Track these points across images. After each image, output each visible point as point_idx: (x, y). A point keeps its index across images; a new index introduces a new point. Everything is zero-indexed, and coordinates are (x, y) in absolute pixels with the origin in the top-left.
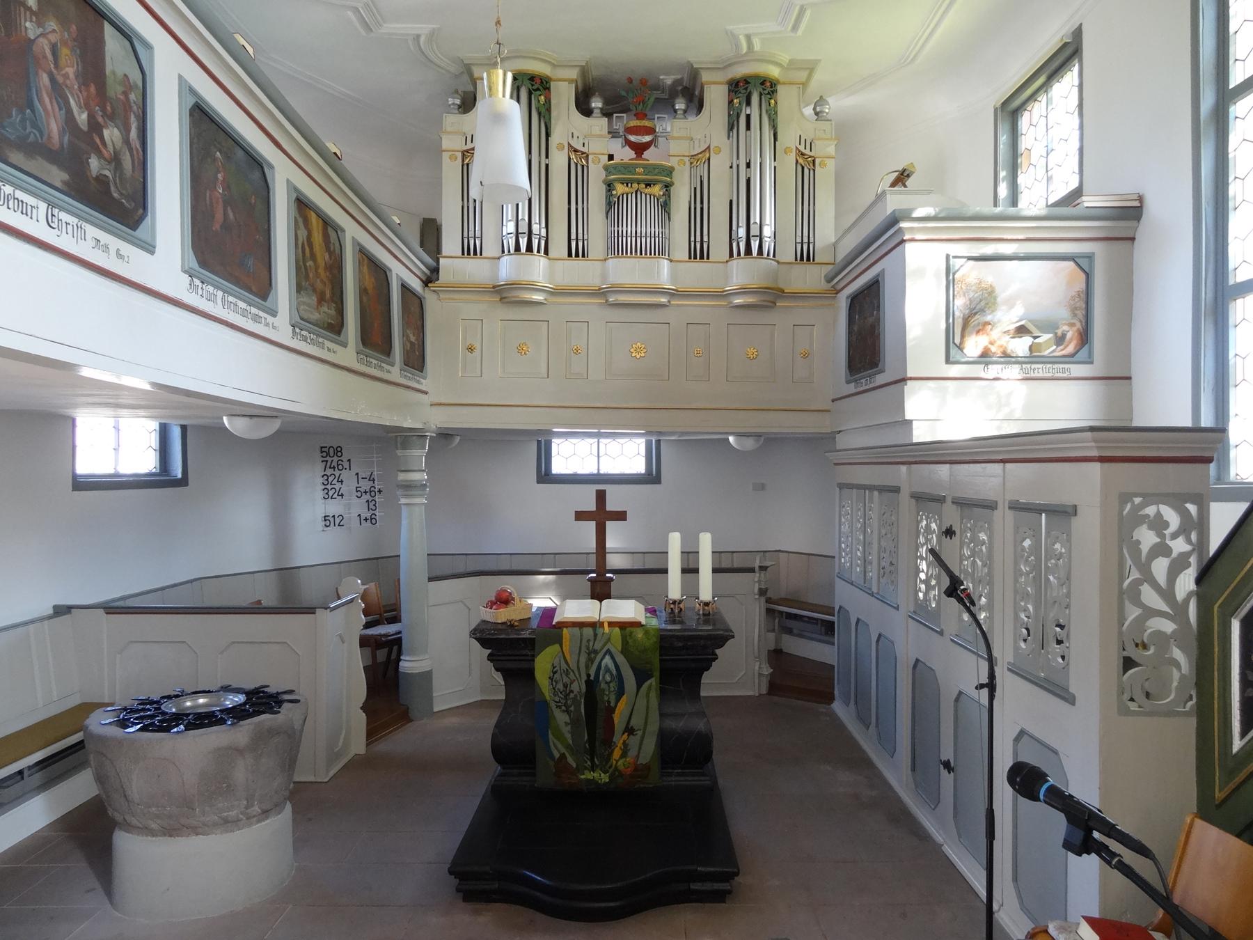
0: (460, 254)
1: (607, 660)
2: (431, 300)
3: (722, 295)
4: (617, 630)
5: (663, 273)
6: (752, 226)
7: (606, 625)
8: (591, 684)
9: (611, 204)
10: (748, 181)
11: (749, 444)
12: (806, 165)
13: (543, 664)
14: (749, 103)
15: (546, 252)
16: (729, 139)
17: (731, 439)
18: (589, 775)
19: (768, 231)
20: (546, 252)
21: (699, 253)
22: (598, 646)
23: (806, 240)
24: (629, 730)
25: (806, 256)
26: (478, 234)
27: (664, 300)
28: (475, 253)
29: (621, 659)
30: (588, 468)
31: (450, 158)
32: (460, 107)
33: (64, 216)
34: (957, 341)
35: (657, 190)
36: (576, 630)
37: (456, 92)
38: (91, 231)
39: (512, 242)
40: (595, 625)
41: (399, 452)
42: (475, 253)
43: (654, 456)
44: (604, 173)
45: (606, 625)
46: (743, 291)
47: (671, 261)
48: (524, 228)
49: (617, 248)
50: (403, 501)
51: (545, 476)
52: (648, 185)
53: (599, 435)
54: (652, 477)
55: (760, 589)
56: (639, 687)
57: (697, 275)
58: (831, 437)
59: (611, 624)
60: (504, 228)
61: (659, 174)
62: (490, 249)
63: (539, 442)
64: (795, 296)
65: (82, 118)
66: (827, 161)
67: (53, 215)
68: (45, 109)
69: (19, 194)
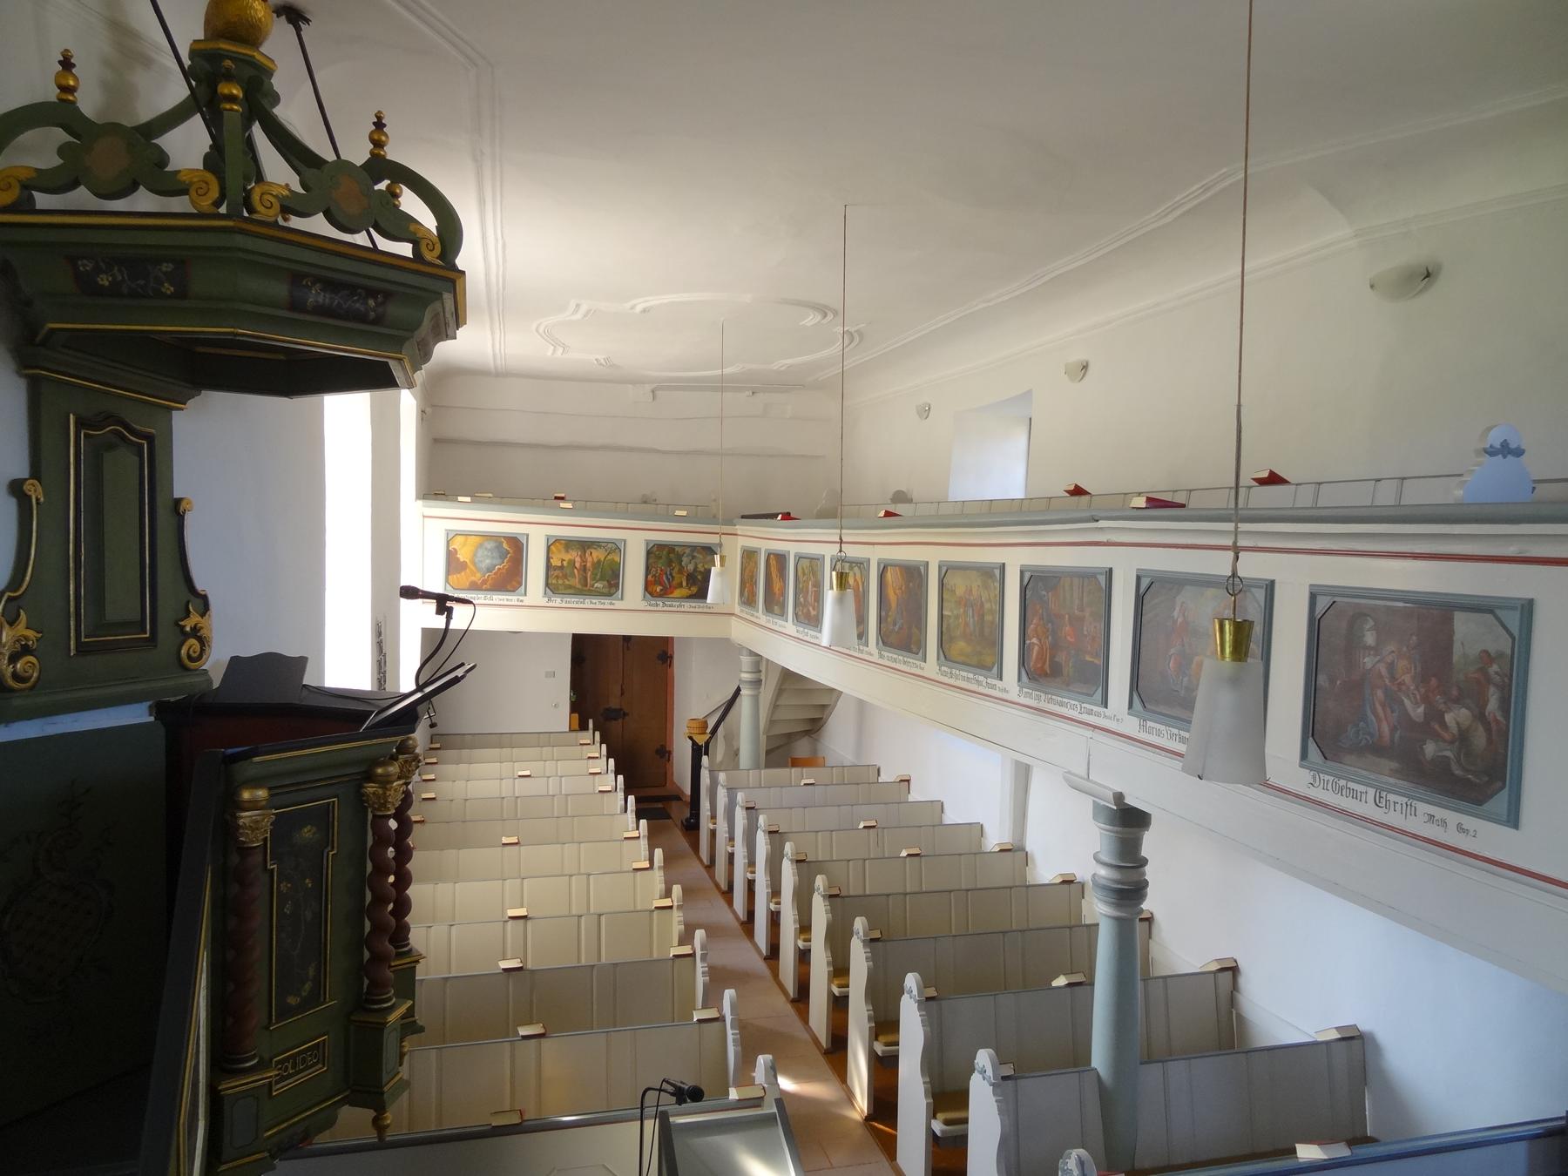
33: (1392, 797)
38: (1423, 808)
65: (1417, 712)
67: (1380, 797)
68: (1377, 716)
69: (1351, 785)
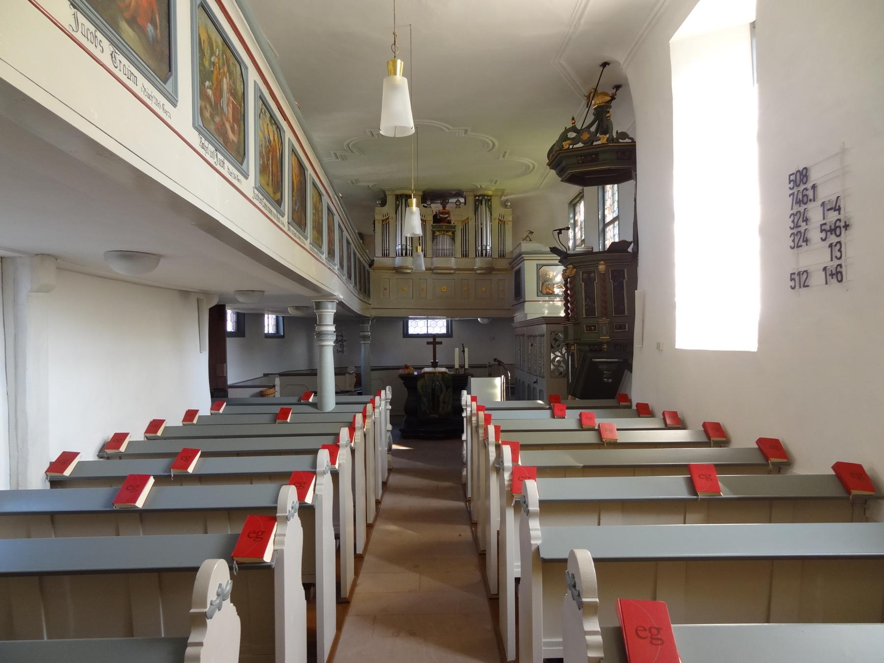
0: (381, 256)
1: (438, 382)
2: (371, 271)
3: (473, 270)
4: (440, 374)
5: (452, 263)
6: (483, 246)
7: (437, 373)
8: (433, 390)
9: (434, 238)
10: (482, 228)
11: (486, 321)
12: (502, 223)
13: (420, 384)
14: (481, 204)
15: (412, 255)
16: (475, 215)
17: (479, 319)
18: (432, 416)
19: (488, 248)
20: (412, 255)
21: (465, 255)
22: (435, 379)
23: (502, 250)
24: (444, 402)
25: (502, 255)
26: (388, 249)
27: (452, 272)
28: (387, 256)
29: (441, 382)
30: (423, 331)
31: (378, 222)
32: (380, 204)
34: (540, 290)
35: (450, 233)
36: (429, 375)
37: (379, 199)
39: (400, 252)
40: (434, 373)
41: (361, 325)
42: (387, 256)
43: (449, 327)
44: (431, 227)
45: (437, 373)
46: (480, 269)
47: (455, 258)
48: (404, 247)
49: (436, 254)
50: (362, 342)
51: (406, 335)
52: (447, 232)
53: (427, 319)
54: (449, 335)
55: (489, 374)
56: (447, 390)
57: (464, 263)
58: (512, 319)
59: (438, 373)
60: (397, 247)
61: (451, 228)
62: (392, 254)
63: (404, 321)
64: (498, 270)
66: (509, 222)
